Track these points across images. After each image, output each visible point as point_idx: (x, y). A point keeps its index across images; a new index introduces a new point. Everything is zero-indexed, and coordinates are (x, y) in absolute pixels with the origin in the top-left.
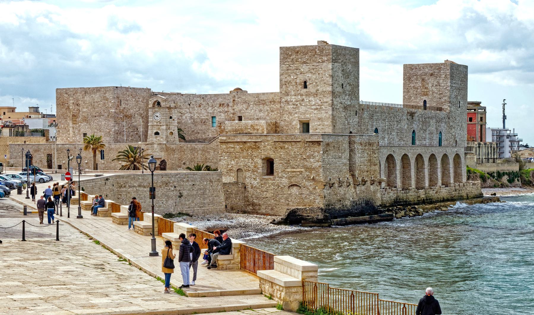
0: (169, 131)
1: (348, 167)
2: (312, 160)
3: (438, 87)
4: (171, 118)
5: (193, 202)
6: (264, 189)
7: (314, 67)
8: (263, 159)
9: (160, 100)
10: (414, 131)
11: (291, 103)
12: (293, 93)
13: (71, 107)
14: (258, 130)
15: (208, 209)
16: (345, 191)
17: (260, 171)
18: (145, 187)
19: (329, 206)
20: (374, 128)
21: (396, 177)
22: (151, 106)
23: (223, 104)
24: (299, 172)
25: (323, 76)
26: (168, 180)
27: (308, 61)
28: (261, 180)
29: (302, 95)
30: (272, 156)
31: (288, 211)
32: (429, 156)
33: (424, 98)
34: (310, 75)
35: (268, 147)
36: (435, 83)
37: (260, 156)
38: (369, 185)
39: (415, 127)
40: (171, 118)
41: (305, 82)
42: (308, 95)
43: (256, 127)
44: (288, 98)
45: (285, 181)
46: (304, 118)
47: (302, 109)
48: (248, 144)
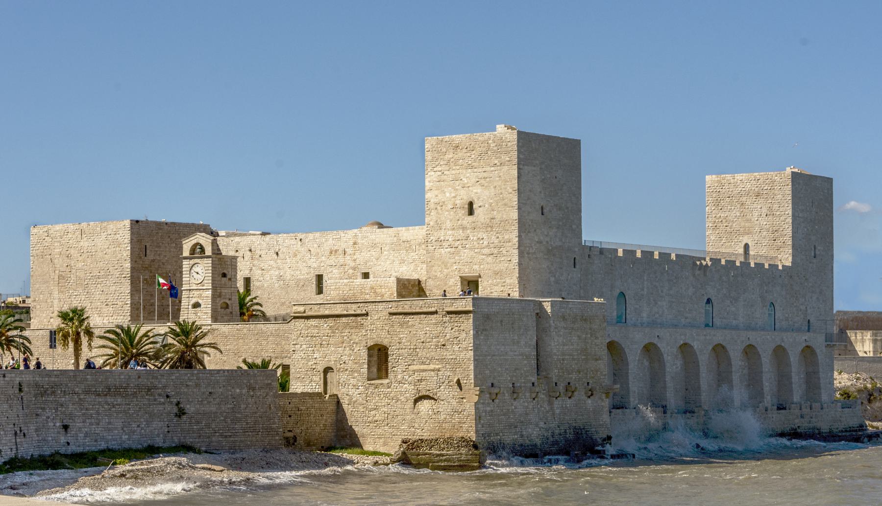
0: (220, 302)
1: (534, 362)
2: (456, 348)
3: (770, 218)
4: (224, 275)
5: (208, 426)
6: (371, 405)
7: (485, 175)
8: (370, 349)
9: (201, 242)
10: (709, 301)
11: (446, 244)
12: (449, 224)
13: (56, 261)
14: (383, 296)
15: (241, 441)
16: (527, 407)
17: (365, 370)
18: (99, 395)
19: (489, 436)
20: (617, 292)
21: (665, 387)
22: (186, 253)
23: (336, 251)
24: (433, 370)
25: (503, 191)
26: (152, 383)
28: (367, 389)
29: (464, 228)
30: (385, 342)
31: (405, 446)
32: (741, 347)
33: (746, 239)
34: (478, 190)
35: (379, 324)
36: (765, 211)
37: (364, 343)
38: (584, 397)
39: (711, 292)
40: (224, 275)
41: (471, 204)
43: (378, 291)
44: (441, 234)
45: (410, 391)
46: (468, 272)
47: (466, 254)
48: (344, 320)
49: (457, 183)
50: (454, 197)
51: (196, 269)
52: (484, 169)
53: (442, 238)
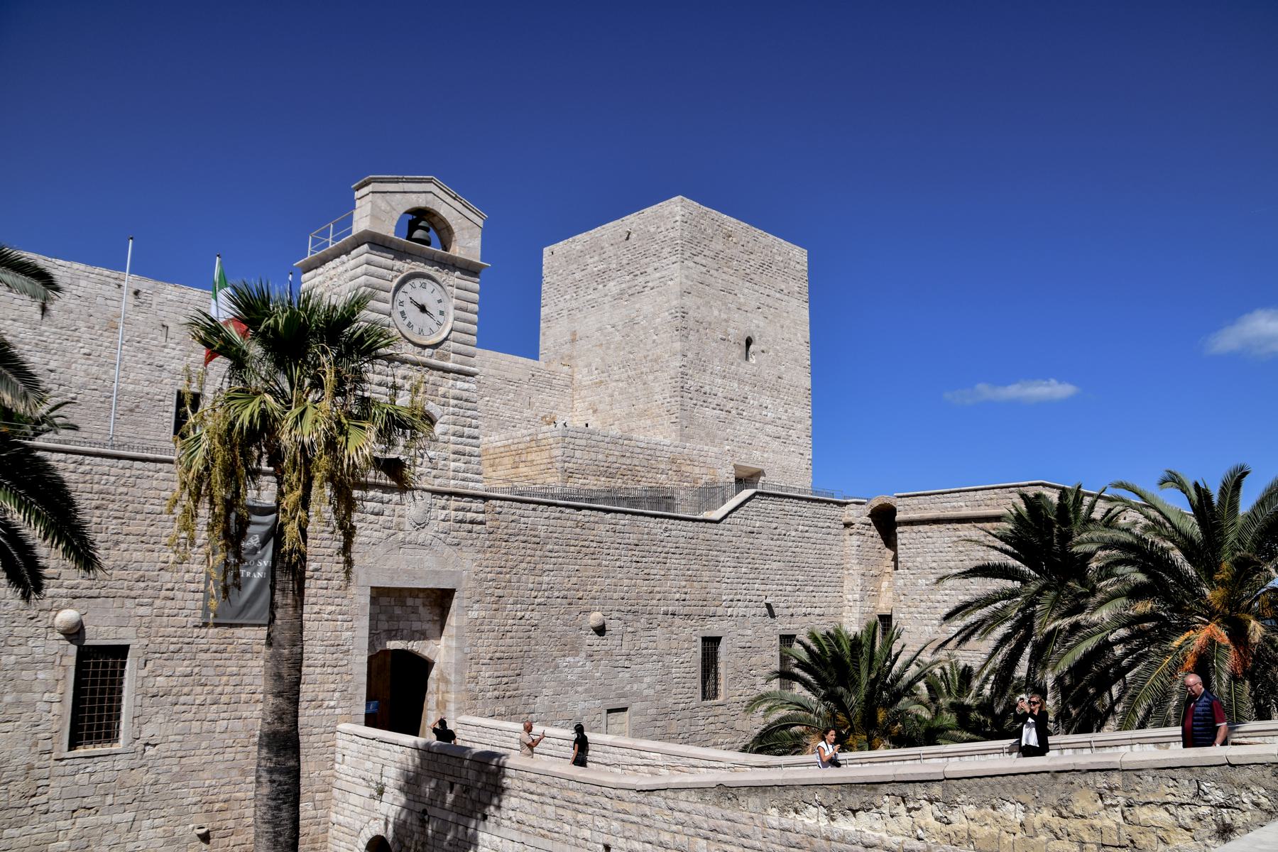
27: (756, 278)
41: (749, 342)
42: (758, 384)
46: (753, 459)
47: (743, 428)
49: (731, 297)
50: (726, 321)
51: (417, 291)
52: (767, 292)
53: (707, 388)
